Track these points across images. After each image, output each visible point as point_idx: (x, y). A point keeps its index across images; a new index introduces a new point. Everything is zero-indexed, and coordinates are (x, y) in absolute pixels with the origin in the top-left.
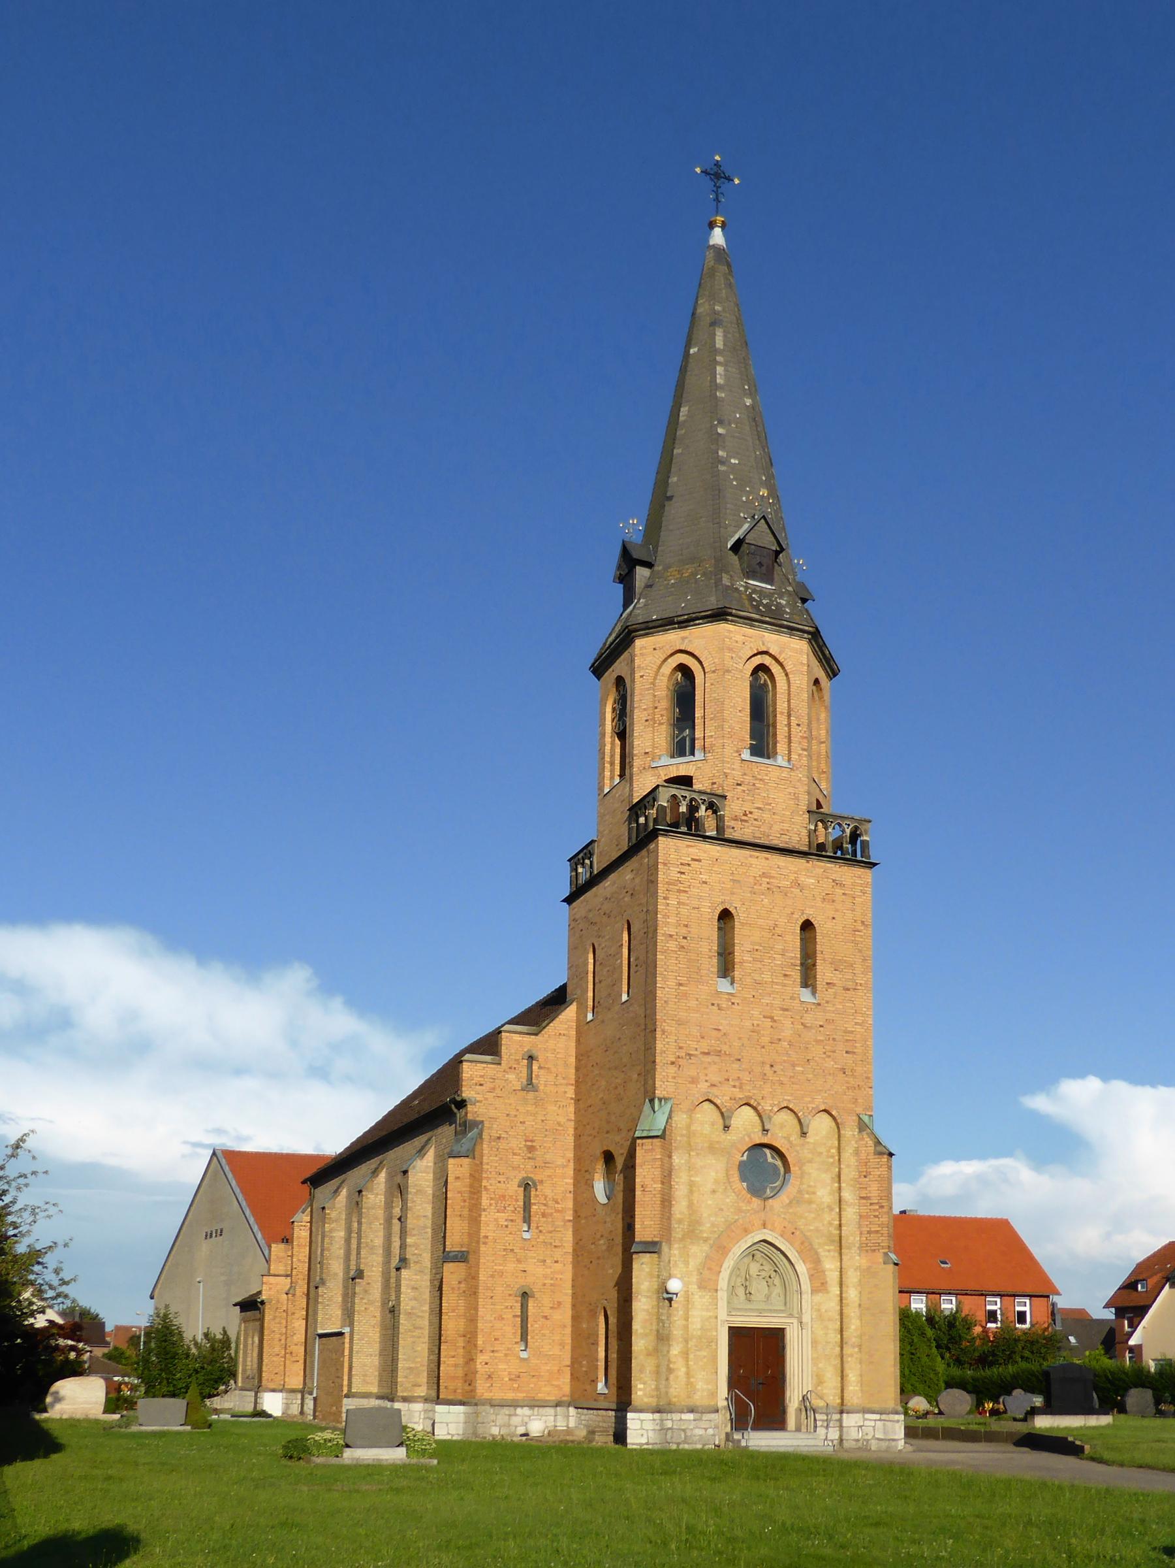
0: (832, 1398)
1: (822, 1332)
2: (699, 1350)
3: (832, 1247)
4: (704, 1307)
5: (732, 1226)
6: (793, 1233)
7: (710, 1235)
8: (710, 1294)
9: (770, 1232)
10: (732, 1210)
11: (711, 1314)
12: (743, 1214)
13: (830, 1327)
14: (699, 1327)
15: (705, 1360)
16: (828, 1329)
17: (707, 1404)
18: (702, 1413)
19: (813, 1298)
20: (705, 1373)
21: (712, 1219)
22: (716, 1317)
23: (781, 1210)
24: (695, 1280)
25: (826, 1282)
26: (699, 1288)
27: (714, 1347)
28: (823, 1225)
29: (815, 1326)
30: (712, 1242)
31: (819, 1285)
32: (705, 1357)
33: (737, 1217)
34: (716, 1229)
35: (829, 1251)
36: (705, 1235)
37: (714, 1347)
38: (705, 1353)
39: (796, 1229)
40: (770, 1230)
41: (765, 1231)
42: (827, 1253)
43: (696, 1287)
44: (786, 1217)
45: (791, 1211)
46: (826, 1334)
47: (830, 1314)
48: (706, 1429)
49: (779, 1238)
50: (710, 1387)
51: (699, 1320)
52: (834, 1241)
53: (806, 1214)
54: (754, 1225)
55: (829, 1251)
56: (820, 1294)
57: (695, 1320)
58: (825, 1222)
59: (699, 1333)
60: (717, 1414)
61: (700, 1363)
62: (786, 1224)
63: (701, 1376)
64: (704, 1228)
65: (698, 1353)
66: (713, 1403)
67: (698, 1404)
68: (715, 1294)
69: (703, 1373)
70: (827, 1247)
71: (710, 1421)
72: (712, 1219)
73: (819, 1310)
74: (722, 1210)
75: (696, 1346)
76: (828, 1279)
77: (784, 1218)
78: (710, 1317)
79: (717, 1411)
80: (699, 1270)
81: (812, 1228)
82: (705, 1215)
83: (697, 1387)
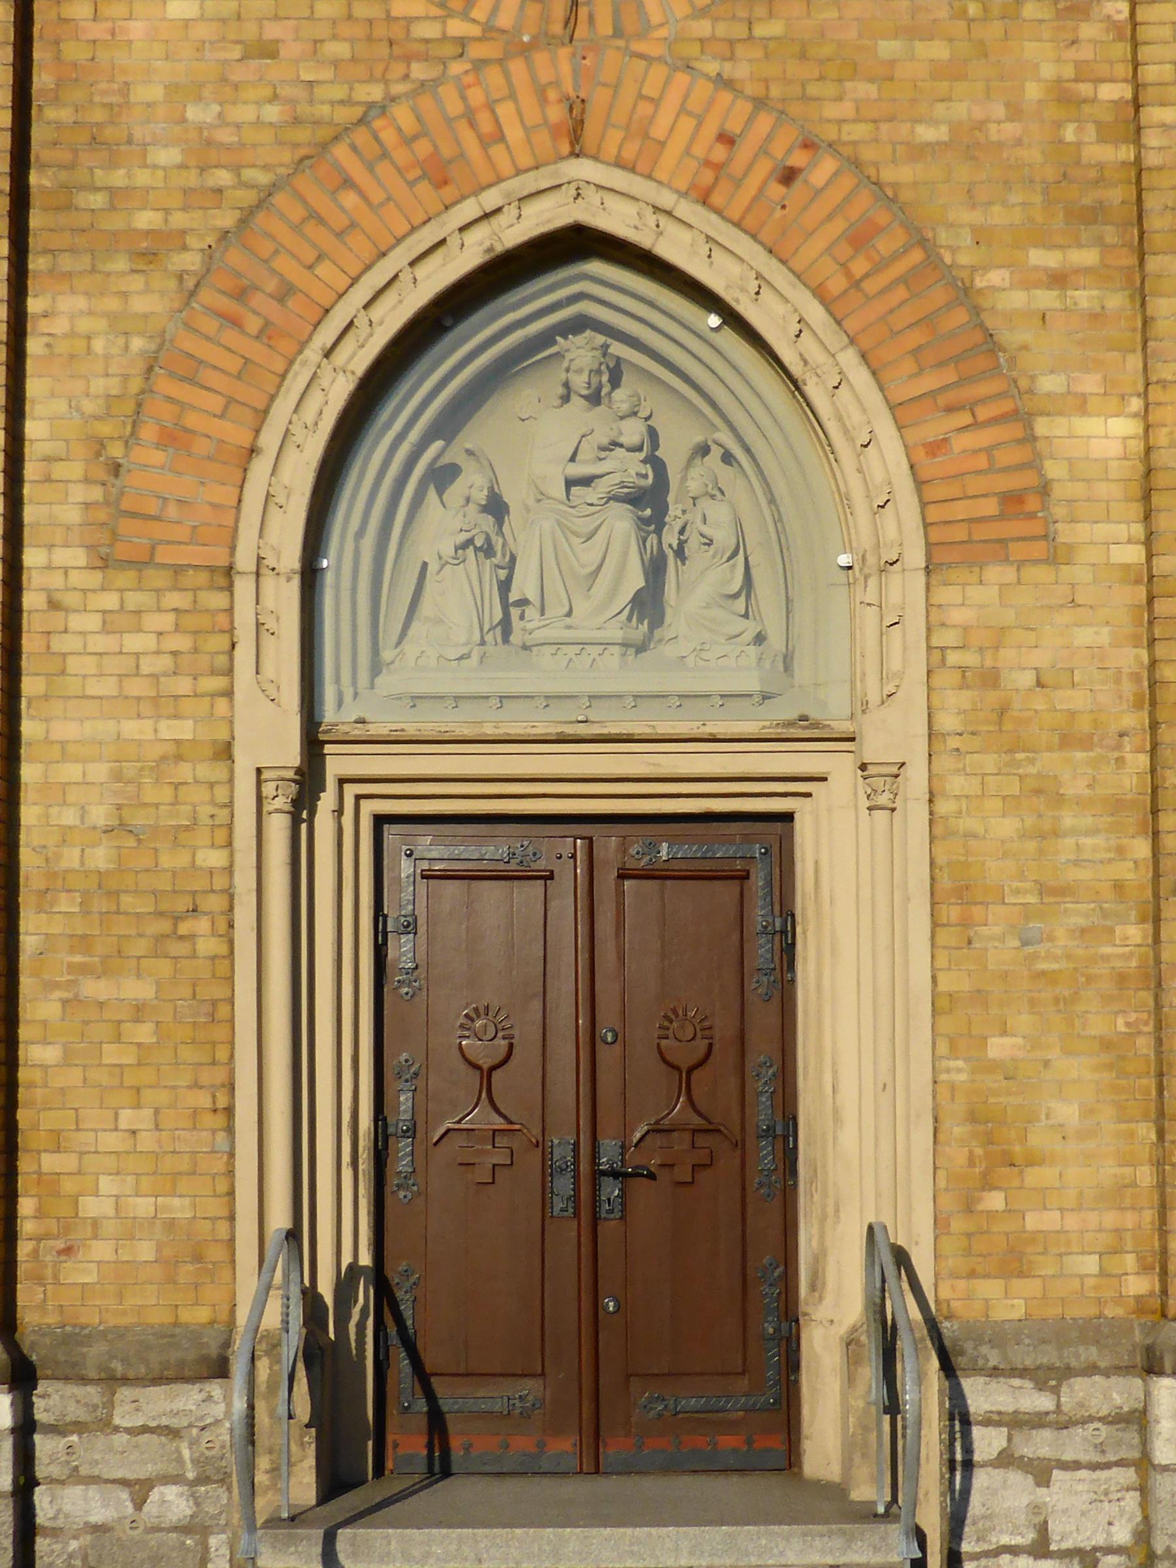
0: (1090, 1264)
1: (1006, 827)
2: (104, 970)
3: (1087, 257)
4: (136, 687)
5: (341, 152)
6: (789, 176)
7: (179, 220)
8: (175, 599)
9: (618, 179)
10: (340, 49)
11: (184, 730)
12: (419, 71)
13: (1075, 787)
14: (100, 815)
15: (144, 1033)
16: (1059, 800)
17: (159, 1317)
18: (112, 1381)
19: (946, 595)
20: (141, 1119)
21: (194, 113)
22: (225, 752)
23: (703, 28)
24: (73, 515)
25: (1044, 490)
26: (104, 563)
27: (208, 946)
28: (1015, 112)
29: (957, 784)
30: (191, 261)
31: (990, 507)
32: (139, 1011)
33: (376, 93)
34: (223, 177)
35: (1059, 280)
36: (146, 219)
37: (208, 946)
38: (140, 990)
39: (808, 145)
40: (619, 164)
41: (583, 169)
42: (1046, 299)
43: (77, 557)
44: (740, 71)
45: (766, 29)
46: (1048, 835)
47: (1076, 699)
48: (140, 1490)
49: (686, 209)
50: (179, 1207)
51: (99, 771)
52: (1094, 215)
53: (888, 48)
54: (499, 137)
55: (1059, 280)
56: (996, 573)
57: (72, 772)
58: (1033, 91)
59: (101, 857)
60: (215, 1388)
61: (112, 1054)
62: (736, 115)
63: (111, 1141)
64: (143, 178)
65: (93, 988)
66: (202, 1315)
67: (90, 1318)
68: (218, 600)
69: (127, 1117)
70: (1043, 258)
71: (173, 1433)
72: (194, 113)
73: (990, 679)
74: (268, 51)
75: (82, 942)
76: (1054, 470)
77: (723, 82)
78: (179, 752)
79: (220, 1369)
80: (99, 445)
81: (926, 134)
82: (149, 92)
83: (91, 1207)
